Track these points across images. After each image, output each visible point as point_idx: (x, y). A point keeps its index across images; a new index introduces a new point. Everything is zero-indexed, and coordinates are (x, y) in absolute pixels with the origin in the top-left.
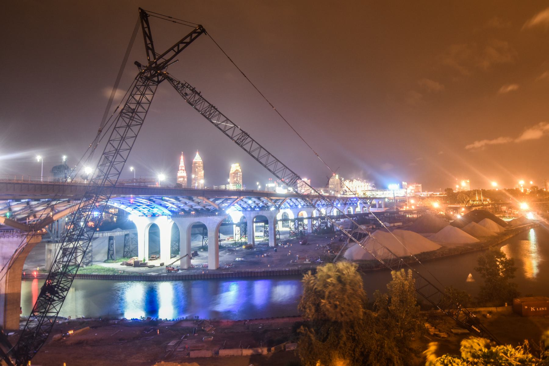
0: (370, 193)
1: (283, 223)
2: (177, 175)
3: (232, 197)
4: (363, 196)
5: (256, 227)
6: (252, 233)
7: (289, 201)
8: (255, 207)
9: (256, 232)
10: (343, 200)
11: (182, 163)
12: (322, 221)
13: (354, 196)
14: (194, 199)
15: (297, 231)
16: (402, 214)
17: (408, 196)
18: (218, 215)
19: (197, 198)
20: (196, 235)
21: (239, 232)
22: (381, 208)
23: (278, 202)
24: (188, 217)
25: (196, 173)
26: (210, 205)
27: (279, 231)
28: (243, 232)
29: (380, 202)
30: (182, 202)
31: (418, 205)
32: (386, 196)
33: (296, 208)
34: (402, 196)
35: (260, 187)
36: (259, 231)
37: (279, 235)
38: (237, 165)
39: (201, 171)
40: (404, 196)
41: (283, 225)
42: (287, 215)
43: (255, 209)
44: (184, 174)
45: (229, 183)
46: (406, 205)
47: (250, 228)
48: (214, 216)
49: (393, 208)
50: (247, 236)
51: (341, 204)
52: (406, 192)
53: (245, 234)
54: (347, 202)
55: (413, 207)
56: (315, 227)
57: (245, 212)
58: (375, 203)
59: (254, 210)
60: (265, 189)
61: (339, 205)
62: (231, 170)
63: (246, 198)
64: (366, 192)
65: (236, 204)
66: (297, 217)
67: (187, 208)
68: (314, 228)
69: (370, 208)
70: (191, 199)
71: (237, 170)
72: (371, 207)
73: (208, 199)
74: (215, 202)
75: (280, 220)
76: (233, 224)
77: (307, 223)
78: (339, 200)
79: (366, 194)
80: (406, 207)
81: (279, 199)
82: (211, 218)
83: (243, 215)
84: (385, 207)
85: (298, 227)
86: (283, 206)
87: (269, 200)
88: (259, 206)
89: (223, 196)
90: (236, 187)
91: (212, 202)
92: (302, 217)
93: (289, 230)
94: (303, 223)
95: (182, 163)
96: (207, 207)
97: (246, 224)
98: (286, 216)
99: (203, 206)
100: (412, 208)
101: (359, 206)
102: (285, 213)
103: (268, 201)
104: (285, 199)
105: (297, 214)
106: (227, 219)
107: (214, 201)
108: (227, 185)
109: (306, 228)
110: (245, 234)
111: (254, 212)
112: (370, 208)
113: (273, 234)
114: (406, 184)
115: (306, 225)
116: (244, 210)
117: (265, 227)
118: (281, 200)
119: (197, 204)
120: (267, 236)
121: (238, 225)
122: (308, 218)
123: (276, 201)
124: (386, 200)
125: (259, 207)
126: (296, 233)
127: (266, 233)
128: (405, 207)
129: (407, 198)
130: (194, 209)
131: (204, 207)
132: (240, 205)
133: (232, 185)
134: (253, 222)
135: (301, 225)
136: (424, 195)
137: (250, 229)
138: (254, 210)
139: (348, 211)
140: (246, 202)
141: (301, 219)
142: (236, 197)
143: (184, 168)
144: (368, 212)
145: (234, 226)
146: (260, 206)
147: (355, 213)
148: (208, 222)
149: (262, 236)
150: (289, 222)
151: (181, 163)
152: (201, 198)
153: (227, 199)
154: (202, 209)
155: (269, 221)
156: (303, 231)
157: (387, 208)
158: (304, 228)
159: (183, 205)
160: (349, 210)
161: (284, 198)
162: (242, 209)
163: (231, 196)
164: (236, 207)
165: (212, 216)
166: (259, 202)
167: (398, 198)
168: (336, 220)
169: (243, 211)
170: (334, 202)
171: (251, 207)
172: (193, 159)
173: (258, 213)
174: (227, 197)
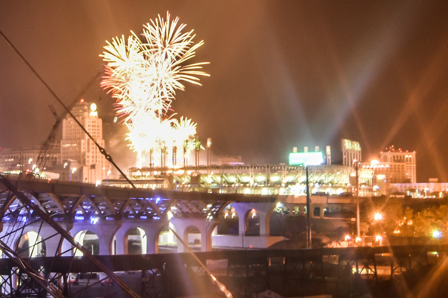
0: (218, 179)
4: (189, 189)
10: (113, 201)
12: (25, 276)
13: (153, 187)
16: (336, 263)
17: (361, 194)
29: (254, 213)
31: (397, 232)
32: (276, 192)
34: (339, 191)
40: (347, 195)
46: (352, 229)
49: (303, 239)
51: (102, 217)
52: (355, 181)
54: (127, 209)
55: (379, 238)
58: (234, 215)
61: (95, 220)
64: (202, 172)
69: (214, 234)
72: (219, 232)
78: (98, 199)
79: (202, 179)
80: (354, 237)
84: (273, 233)
100: (373, 242)
112: (214, 234)
114: (357, 147)
124: (279, 206)
128: (347, 237)
129: (358, 202)
136: (422, 193)
139: (131, 242)
144: (204, 250)
147: (157, 252)
157: (281, 238)
160: (130, 237)
167: (323, 200)
168: (81, 277)
170: (74, 204)
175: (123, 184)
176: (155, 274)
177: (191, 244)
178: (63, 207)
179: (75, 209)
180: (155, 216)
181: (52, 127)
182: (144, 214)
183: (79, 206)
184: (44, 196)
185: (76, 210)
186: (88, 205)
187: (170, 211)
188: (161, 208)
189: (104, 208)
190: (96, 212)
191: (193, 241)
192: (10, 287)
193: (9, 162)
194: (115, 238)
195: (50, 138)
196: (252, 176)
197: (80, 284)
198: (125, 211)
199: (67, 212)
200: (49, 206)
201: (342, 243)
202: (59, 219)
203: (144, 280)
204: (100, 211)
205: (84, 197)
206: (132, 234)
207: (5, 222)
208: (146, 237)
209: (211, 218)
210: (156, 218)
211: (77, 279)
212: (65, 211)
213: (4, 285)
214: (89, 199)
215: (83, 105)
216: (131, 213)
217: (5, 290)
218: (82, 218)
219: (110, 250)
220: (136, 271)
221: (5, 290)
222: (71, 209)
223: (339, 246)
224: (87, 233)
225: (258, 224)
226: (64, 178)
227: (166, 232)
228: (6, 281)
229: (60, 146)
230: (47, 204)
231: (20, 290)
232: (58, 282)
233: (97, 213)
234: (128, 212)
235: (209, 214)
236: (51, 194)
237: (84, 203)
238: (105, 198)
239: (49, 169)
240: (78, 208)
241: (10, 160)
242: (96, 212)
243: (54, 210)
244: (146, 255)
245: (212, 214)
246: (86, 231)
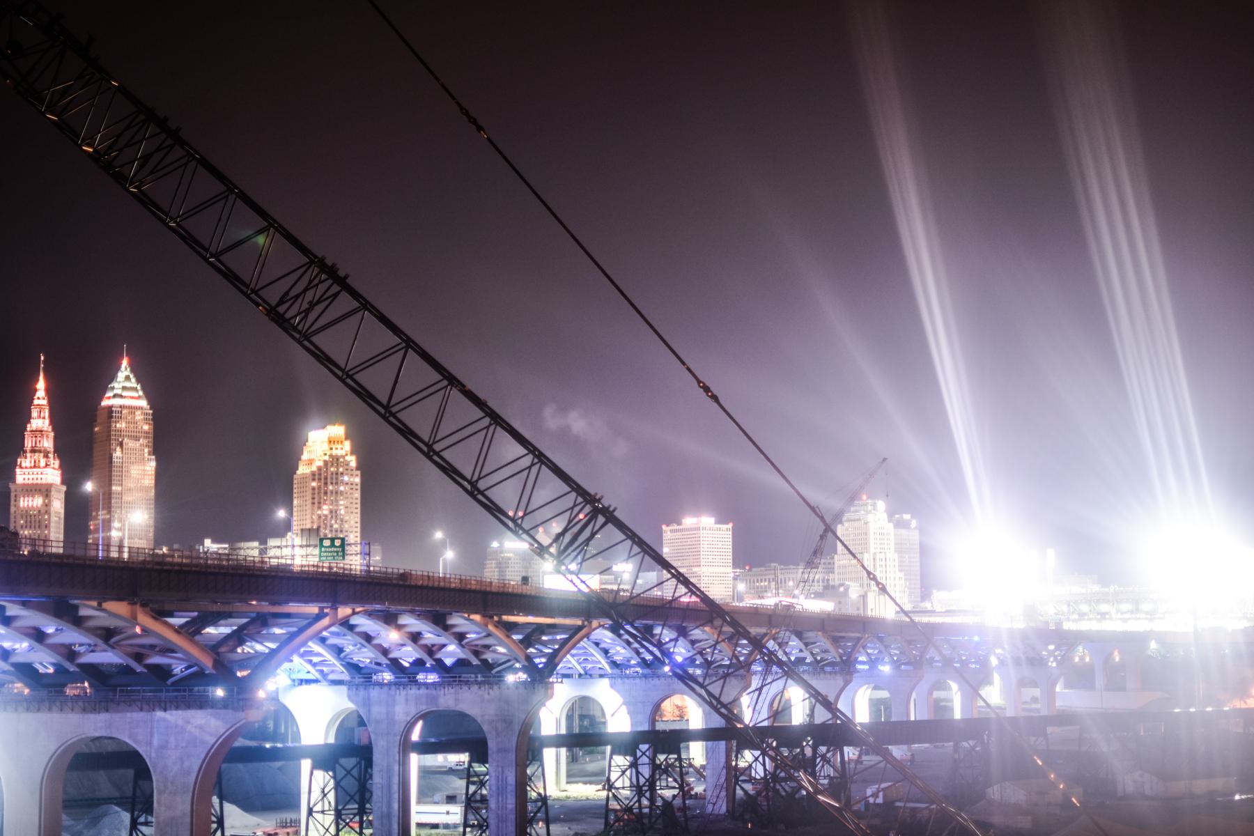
1: (573, 759)
2: (13, 478)
3: (293, 607)
5: (425, 772)
6: (396, 806)
7: (605, 636)
8: (419, 663)
9: (419, 802)
10: (910, 642)
11: (40, 421)
14: (83, 612)
15: (645, 802)
18: (225, 704)
19: (100, 608)
20: (99, 811)
21: (331, 797)
22: (1123, 689)
23: (545, 644)
24: (50, 709)
25: (107, 472)
26: (168, 650)
27: (543, 799)
28: (352, 798)
30: (18, 630)
33: (645, 676)
35: (450, 555)
36: (437, 797)
37: (548, 822)
38: (338, 430)
39: (142, 461)
41: (576, 767)
42: (597, 713)
43: (420, 677)
44: (52, 475)
45: (283, 529)
47: (390, 778)
48: (189, 706)
50: (370, 824)
51: (896, 665)
53: (362, 811)
56: (748, 787)
57: (362, 692)
59: (414, 681)
60: (482, 566)
61: (886, 669)
62: (305, 457)
63: (370, 614)
65: (315, 647)
66: (645, 727)
67: (45, 662)
68: (739, 792)
70: (66, 613)
71: (335, 460)
72: (1068, 685)
73: (160, 614)
74: (198, 632)
75: (558, 741)
76: (291, 756)
77: (705, 763)
81: (552, 628)
82: (174, 717)
83: (351, 706)
85: (652, 784)
86: (570, 661)
87: (491, 627)
88: (440, 662)
89: (245, 601)
90: (316, 551)
91: (179, 630)
92: (677, 727)
93: (604, 794)
94: (679, 759)
95: (40, 421)
96: (156, 660)
97: (364, 754)
98: (592, 719)
99: (129, 655)
101: (996, 678)
102: (584, 701)
103: (489, 635)
104: (580, 628)
105: (649, 709)
106: (271, 724)
107: (192, 630)
108: (272, 542)
109: (699, 789)
110: (362, 811)
111: (413, 691)
113: (513, 817)
115: (699, 773)
116: (358, 680)
117: (468, 774)
118: (563, 628)
119: (100, 642)
120: (480, 826)
121: (326, 759)
122: (709, 735)
123: (532, 636)
125: (440, 666)
126: (640, 815)
127: (477, 810)
130: (81, 666)
131: (139, 657)
132: (338, 651)
133: (298, 541)
134: (406, 747)
135: (666, 770)
137: (389, 787)
138: (414, 681)
139: (937, 701)
140: (368, 638)
141: (672, 741)
142: (313, 609)
143: (48, 443)
144: (1044, 712)
145: (306, 764)
146: (448, 662)
147: (976, 716)
148: (156, 742)
149: (455, 826)
150: (604, 753)
151: (35, 414)
152: (120, 608)
153: (262, 621)
154: (126, 670)
155: (492, 745)
156: (677, 802)
158: (684, 788)
159: (25, 645)
160: (936, 694)
161: (579, 622)
162: (346, 676)
163: (287, 602)
164: (315, 659)
165: (177, 708)
166: (442, 640)
168: (867, 754)
169: (349, 684)
171: (395, 665)
172: (101, 398)
173: (434, 699)
174: (266, 607)
175: (925, 616)
176: (973, 748)
177: (1026, 703)
178: (838, 651)
179: (855, 654)
180: (972, 663)
181: (819, 538)
182: (956, 660)
183: (861, 649)
184: (811, 635)
185: (857, 656)
186: (874, 648)
187: (995, 656)
188: (980, 652)
189: (898, 652)
190: (886, 658)
191: (1029, 701)
192: (762, 767)
193: (762, 586)
194: (914, 696)
195: (815, 553)
196: (1113, 604)
197: (864, 763)
198: (928, 657)
199: (844, 658)
200: (818, 650)
201: (1248, 701)
202: (833, 669)
203: (956, 756)
204: (891, 656)
205: (868, 637)
206: (939, 689)
207: (755, 673)
208: (959, 693)
209: (1054, 665)
210: (973, 666)
211: (860, 756)
212: (841, 657)
213: (754, 765)
214: (875, 640)
215: (866, 505)
216: (937, 658)
217: (756, 772)
218: (866, 667)
219: (908, 714)
220: (946, 744)
221: (756, 772)
222: (849, 655)
223: (1244, 706)
224: (875, 688)
225: (1123, 674)
226: (840, 609)
227: (988, 686)
228: (756, 759)
229: (834, 563)
230: (816, 647)
231: (778, 772)
232: (832, 760)
233: (887, 659)
234: (932, 659)
235: (1052, 659)
236: (820, 633)
237: (869, 645)
238: (898, 638)
239: (818, 596)
240: (860, 652)
241: (762, 584)
242: (886, 658)
243: (825, 656)
244: (963, 720)
245: (1055, 659)
246: (873, 685)
